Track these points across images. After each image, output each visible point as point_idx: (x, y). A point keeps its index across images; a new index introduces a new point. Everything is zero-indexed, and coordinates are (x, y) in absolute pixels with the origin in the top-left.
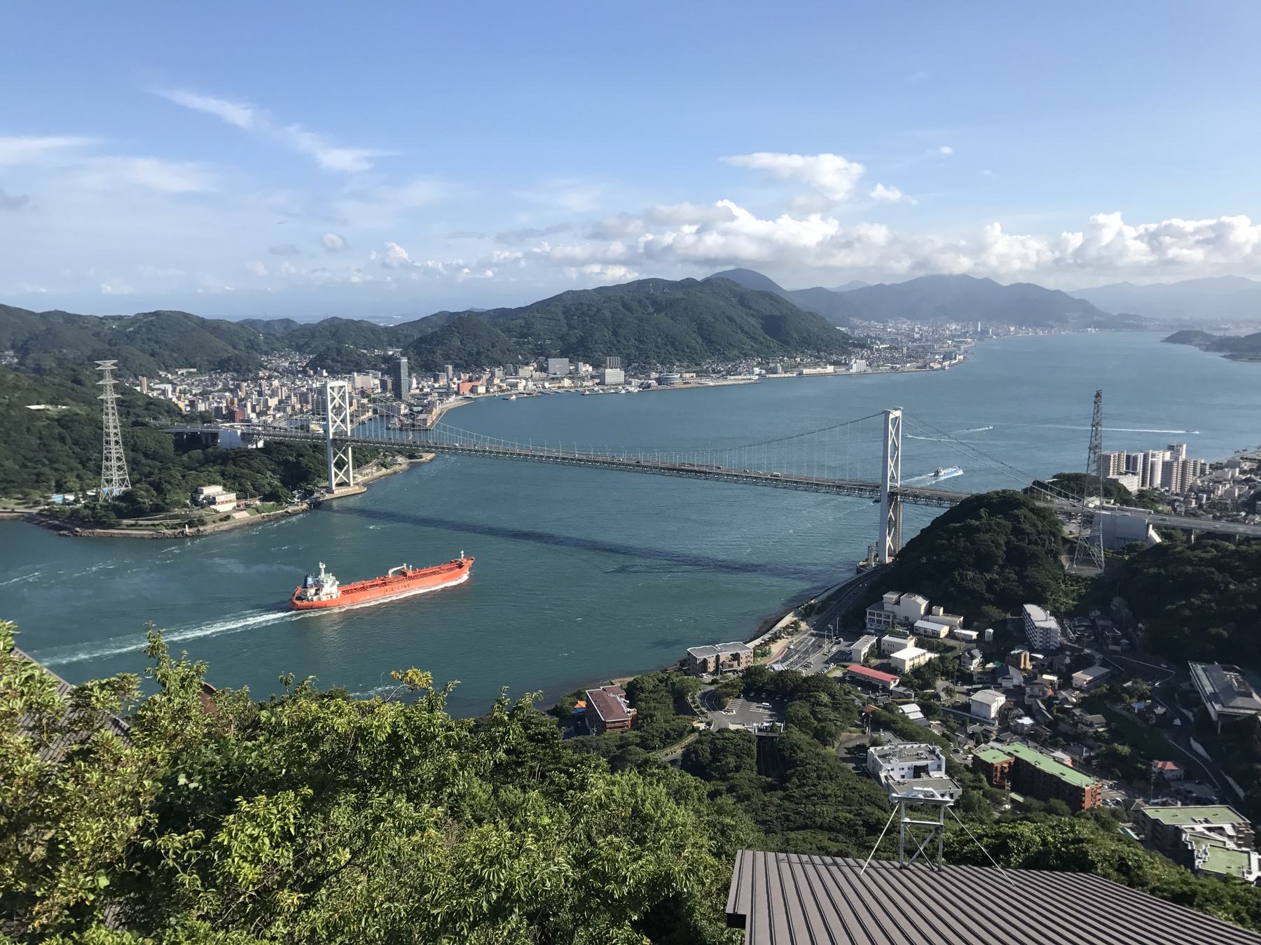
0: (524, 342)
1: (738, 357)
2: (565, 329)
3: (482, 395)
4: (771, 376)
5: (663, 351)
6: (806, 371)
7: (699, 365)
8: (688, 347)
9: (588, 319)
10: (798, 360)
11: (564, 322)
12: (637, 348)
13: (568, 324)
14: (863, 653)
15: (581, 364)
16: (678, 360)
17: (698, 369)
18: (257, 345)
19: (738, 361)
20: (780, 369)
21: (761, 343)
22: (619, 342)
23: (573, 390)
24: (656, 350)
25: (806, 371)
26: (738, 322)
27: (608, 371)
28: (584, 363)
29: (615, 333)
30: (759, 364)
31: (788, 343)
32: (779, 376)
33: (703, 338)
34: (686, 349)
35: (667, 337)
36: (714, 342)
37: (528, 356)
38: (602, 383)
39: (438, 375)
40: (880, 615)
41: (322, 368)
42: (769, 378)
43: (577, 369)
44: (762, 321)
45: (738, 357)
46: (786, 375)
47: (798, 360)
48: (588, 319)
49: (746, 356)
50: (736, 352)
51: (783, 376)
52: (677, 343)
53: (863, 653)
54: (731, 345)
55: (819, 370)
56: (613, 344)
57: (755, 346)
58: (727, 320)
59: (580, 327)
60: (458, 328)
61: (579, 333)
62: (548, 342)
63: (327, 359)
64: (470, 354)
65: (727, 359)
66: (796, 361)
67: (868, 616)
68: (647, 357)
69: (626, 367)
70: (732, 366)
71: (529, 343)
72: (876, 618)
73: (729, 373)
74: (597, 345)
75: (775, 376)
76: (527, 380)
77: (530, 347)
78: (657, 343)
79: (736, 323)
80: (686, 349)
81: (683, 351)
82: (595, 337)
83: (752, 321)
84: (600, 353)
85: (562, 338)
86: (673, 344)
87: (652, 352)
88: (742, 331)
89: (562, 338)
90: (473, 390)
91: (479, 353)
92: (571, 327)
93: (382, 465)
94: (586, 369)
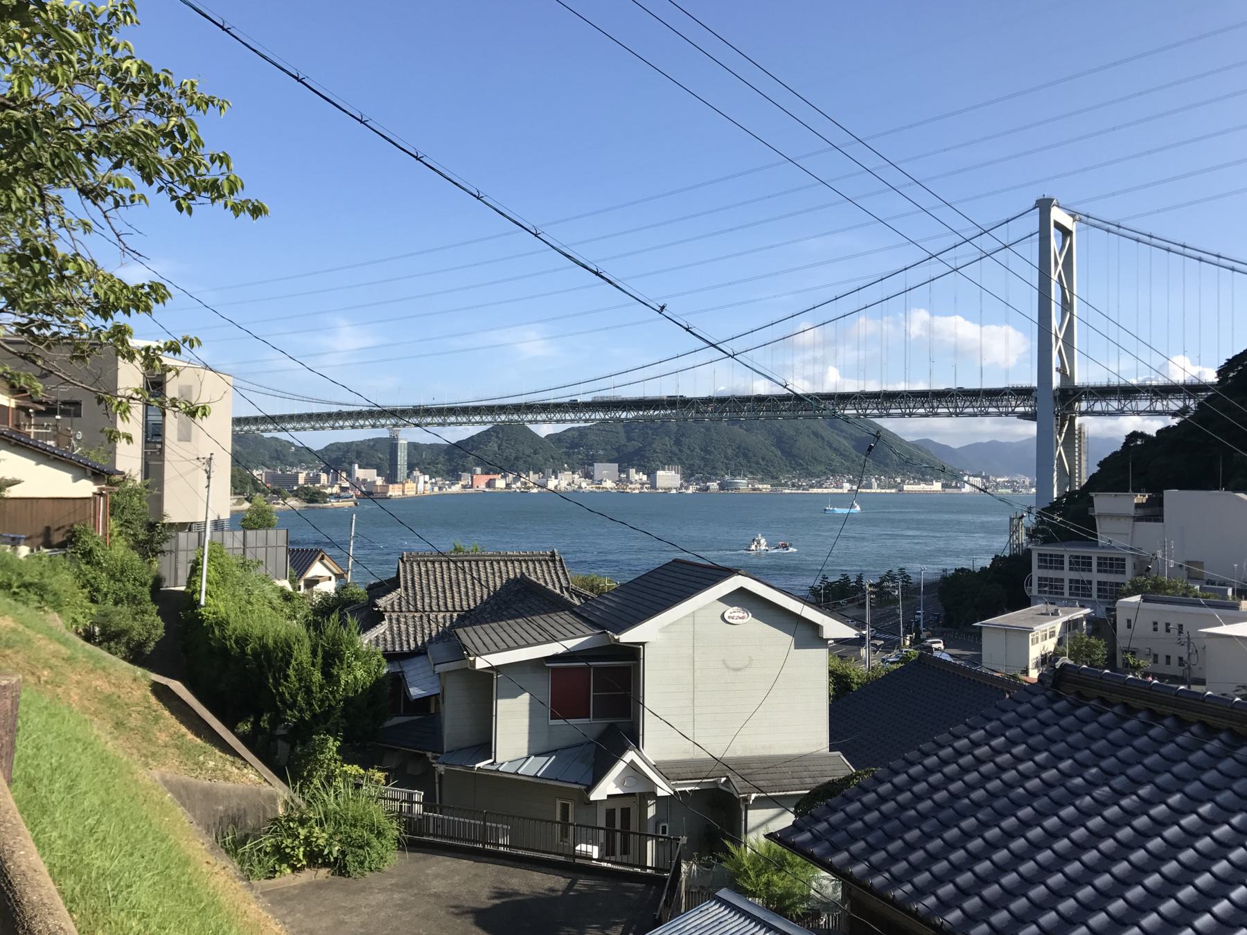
0: (574, 452)
1: (825, 473)
2: (623, 441)
3: (499, 490)
4: (864, 490)
5: (732, 462)
6: (906, 488)
7: (777, 478)
8: (763, 459)
9: (650, 432)
10: (899, 480)
11: (622, 435)
12: (703, 458)
13: (627, 437)
14: (1035, 652)
15: (633, 471)
16: (751, 473)
17: (776, 482)
18: (284, 456)
19: (823, 478)
20: (875, 485)
21: (853, 461)
22: (681, 451)
23: (614, 491)
24: (726, 461)
25: (906, 488)
26: (826, 439)
27: (659, 473)
28: (637, 472)
29: (678, 442)
30: (849, 481)
31: (886, 465)
32: (873, 491)
33: (783, 452)
34: (761, 461)
35: (739, 448)
36: (795, 456)
37: (576, 465)
38: (653, 486)
39: (460, 476)
40: (1084, 564)
41: (342, 471)
42: (861, 493)
43: (628, 477)
44: (854, 443)
45: (825, 473)
46: (883, 491)
47: (899, 480)
48: (650, 432)
49: (834, 472)
50: (822, 468)
51: (879, 491)
52: (751, 454)
53: (1035, 652)
54: (815, 459)
55: (923, 487)
56: (675, 454)
57: (846, 464)
58: (812, 436)
59: (641, 440)
60: (498, 433)
61: (636, 444)
62: (601, 452)
63: (344, 462)
64: (507, 459)
65: (810, 475)
66: (895, 482)
67: (1036, 573)
68: (714, 468)
69: (687, 477)
70: (817, 482)
71: (579, 453)
72: (1067, 574)
73: (812, 486)
74: (655, 455)
75: (868, 491)
76: (561, 482)
77: (580, 457)
78: (726, 452)
79: (823, 439)
80: (761, 461)
81: (757, 463)
82: (654, 446)
83: (845, 443)
84: (659, 463)
85: (618, 450)
86: (745, 455)
87: (719, 463)
88: (831, 447)
89: (618, 450)
90: (490, 484)
91: (517, 459)
92: (629, 439)
93: (247, 499)
94: (638, 477)
